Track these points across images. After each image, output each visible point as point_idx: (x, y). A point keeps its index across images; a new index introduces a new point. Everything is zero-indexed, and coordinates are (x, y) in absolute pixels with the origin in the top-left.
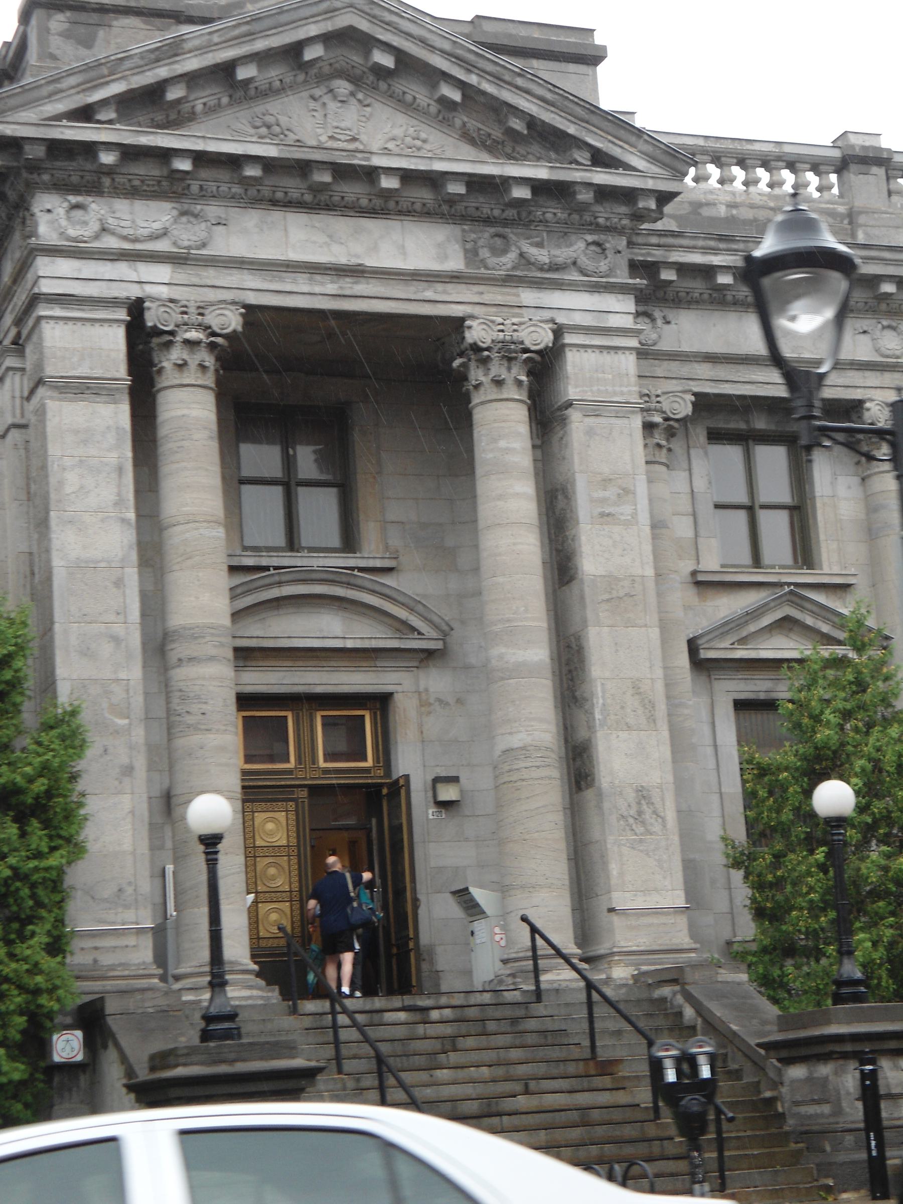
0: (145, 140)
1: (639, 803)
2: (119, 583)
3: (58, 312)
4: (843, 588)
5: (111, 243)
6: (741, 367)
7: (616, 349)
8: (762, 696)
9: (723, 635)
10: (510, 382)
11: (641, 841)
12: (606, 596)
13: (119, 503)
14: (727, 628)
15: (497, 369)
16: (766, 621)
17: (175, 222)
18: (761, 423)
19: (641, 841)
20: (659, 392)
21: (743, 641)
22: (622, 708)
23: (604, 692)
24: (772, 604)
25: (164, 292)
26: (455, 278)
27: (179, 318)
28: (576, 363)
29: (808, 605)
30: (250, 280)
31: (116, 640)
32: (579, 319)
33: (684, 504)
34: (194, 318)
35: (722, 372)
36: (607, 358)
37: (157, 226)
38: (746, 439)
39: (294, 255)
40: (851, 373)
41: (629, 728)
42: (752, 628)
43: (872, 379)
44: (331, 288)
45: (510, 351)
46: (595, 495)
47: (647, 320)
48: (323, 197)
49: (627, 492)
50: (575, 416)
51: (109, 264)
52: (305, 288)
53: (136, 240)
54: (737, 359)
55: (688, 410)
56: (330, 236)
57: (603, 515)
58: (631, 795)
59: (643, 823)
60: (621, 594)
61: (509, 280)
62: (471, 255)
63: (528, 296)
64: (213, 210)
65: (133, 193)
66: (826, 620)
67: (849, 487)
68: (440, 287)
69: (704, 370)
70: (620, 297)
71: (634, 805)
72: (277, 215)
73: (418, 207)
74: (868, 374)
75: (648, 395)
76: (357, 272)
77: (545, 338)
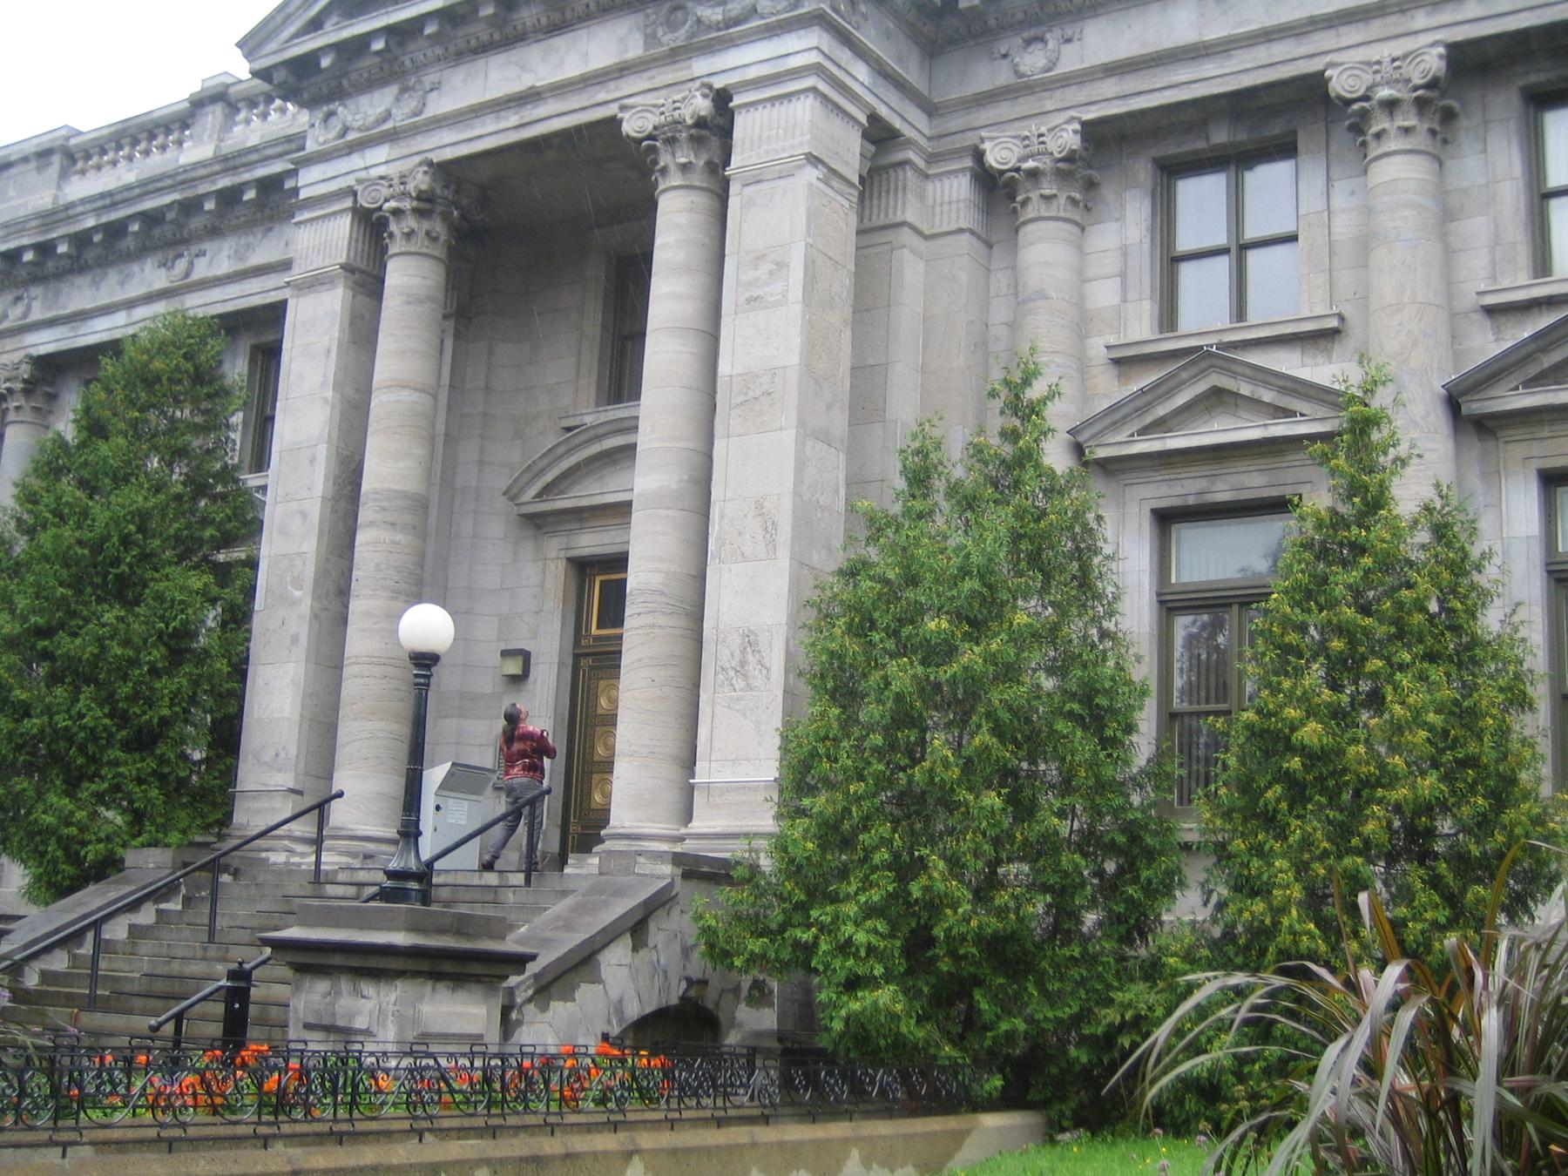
0: (346, 34)
1: (744, 651)
2: (312, 461)
3: (306, 215)
4: (1321, 338)
5: (351, 136)
6: (1157, 71)
7: (788, 96)
8: (1191, 501)
9: (1115, 426)
10: (672, 167)
11: (739, 699)
12: (739, 400)
13: (323, 384)
14: (1117, 416)
15: (664, 159)
16: (1181, 399)
17: (397, 99)
18: (1220, 136)
19: (739, 699)
20: (1043, 130)
21: (1160, 426)
22: (740, 534)
23: (722, 517)
24: (1185, 375)
25: (382, 170)
26: (622, 70)
27: (386, 192)
28: (743, 126)
29: (1235, 367)
30: (448, 136)
31: (304, 515)
32: (752, 73)
33: (1111, 263)
34: (399, 189)
35: (1131, 83)
36: (781, 110)
37: (381, 109)
38: (1236, 160)
39: (488, 97)
40: (1317, 36)
41: (744, 558)
42: (1161, 411)
43: (1351, 34)
44: (513, 119)
45: (668, 135)
46: (743, 278)
47: (1040, 46)
48: (508, 30)
49: (781, 265)
50: (734, 188)
51: (345, 159)
52: (492, 128)
53: (368, 129)
54: (1146, 61)
55: (1070, 139)
56: (523, 68)
57: (750, 300)
58: (735, 641)
59: (745, 676)
60: (758, 393)
61: (676, 55)
62: (651, 39)
63: (700, 66)
64: (429, 78)
65: (372, 84)
66: (1266, 384)
67: (1352, 193)
68: (612, 85)
69: (1110, 87)
70: (802, 32)
71: (738, 654)
72: (480, 63)
73: (593, 7)
74: (1343, 30)
75: (1026, 138)
76: (532, 96)
77: (702, 105)
